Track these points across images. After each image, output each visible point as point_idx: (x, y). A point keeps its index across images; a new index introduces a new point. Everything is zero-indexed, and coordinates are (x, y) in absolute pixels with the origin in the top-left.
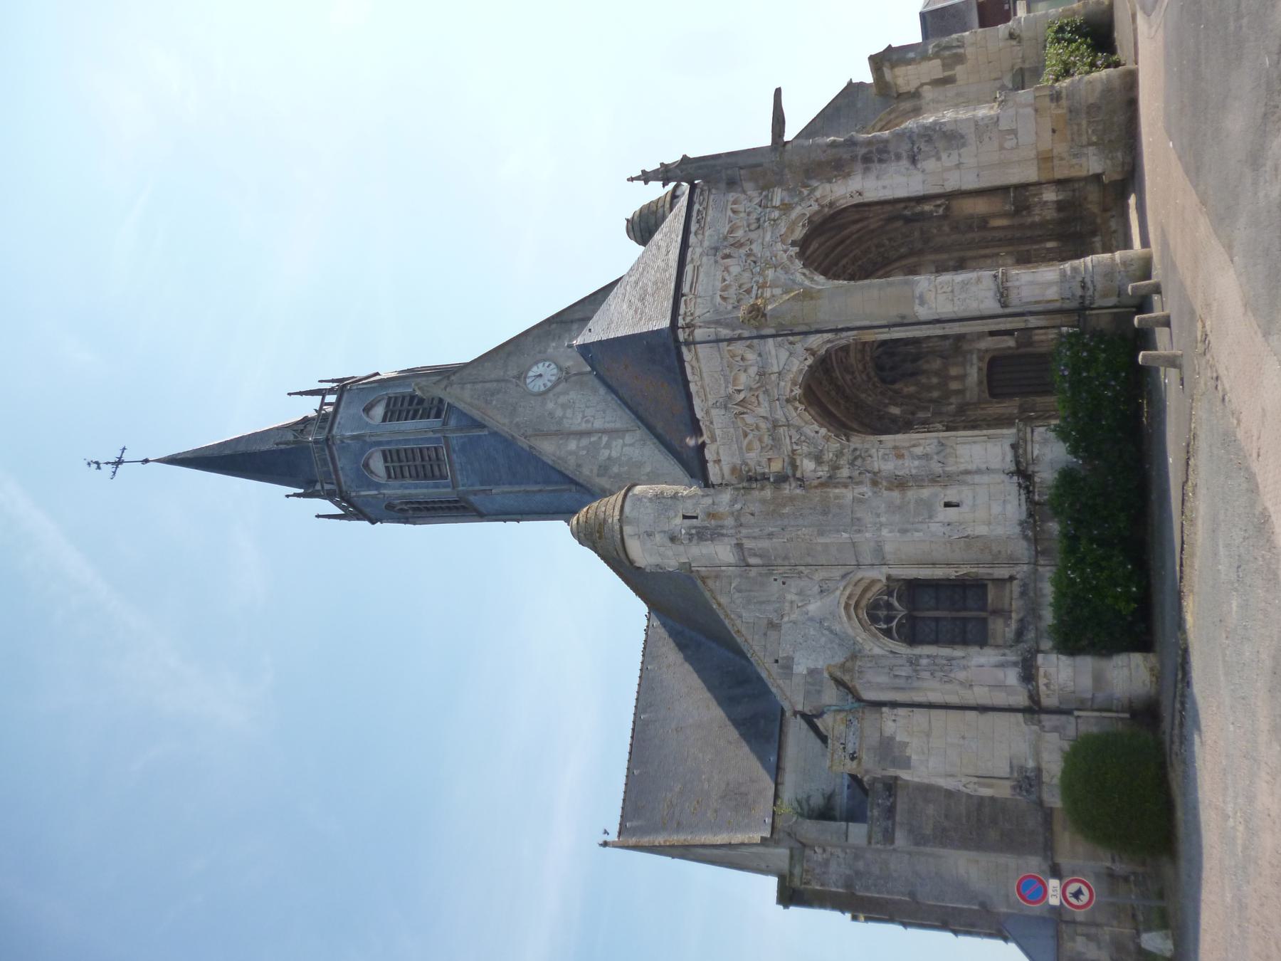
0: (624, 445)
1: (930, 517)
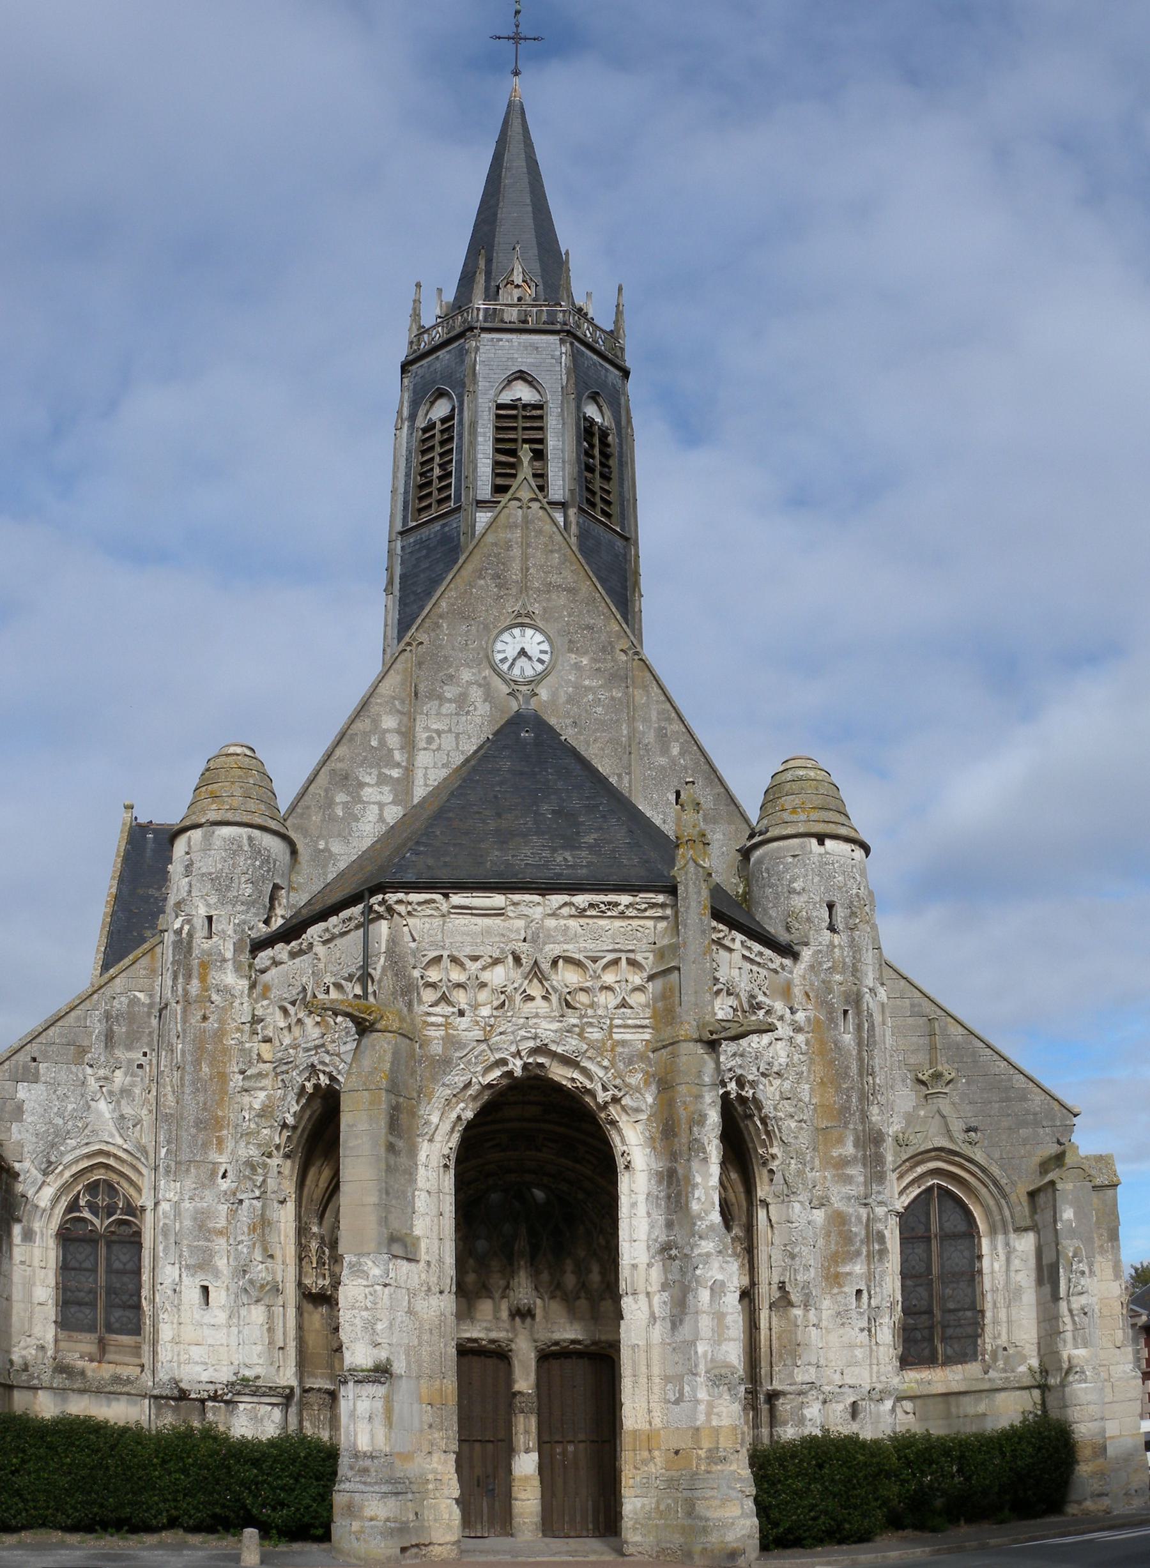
0: (381, 805)
1: (188, 1267)
